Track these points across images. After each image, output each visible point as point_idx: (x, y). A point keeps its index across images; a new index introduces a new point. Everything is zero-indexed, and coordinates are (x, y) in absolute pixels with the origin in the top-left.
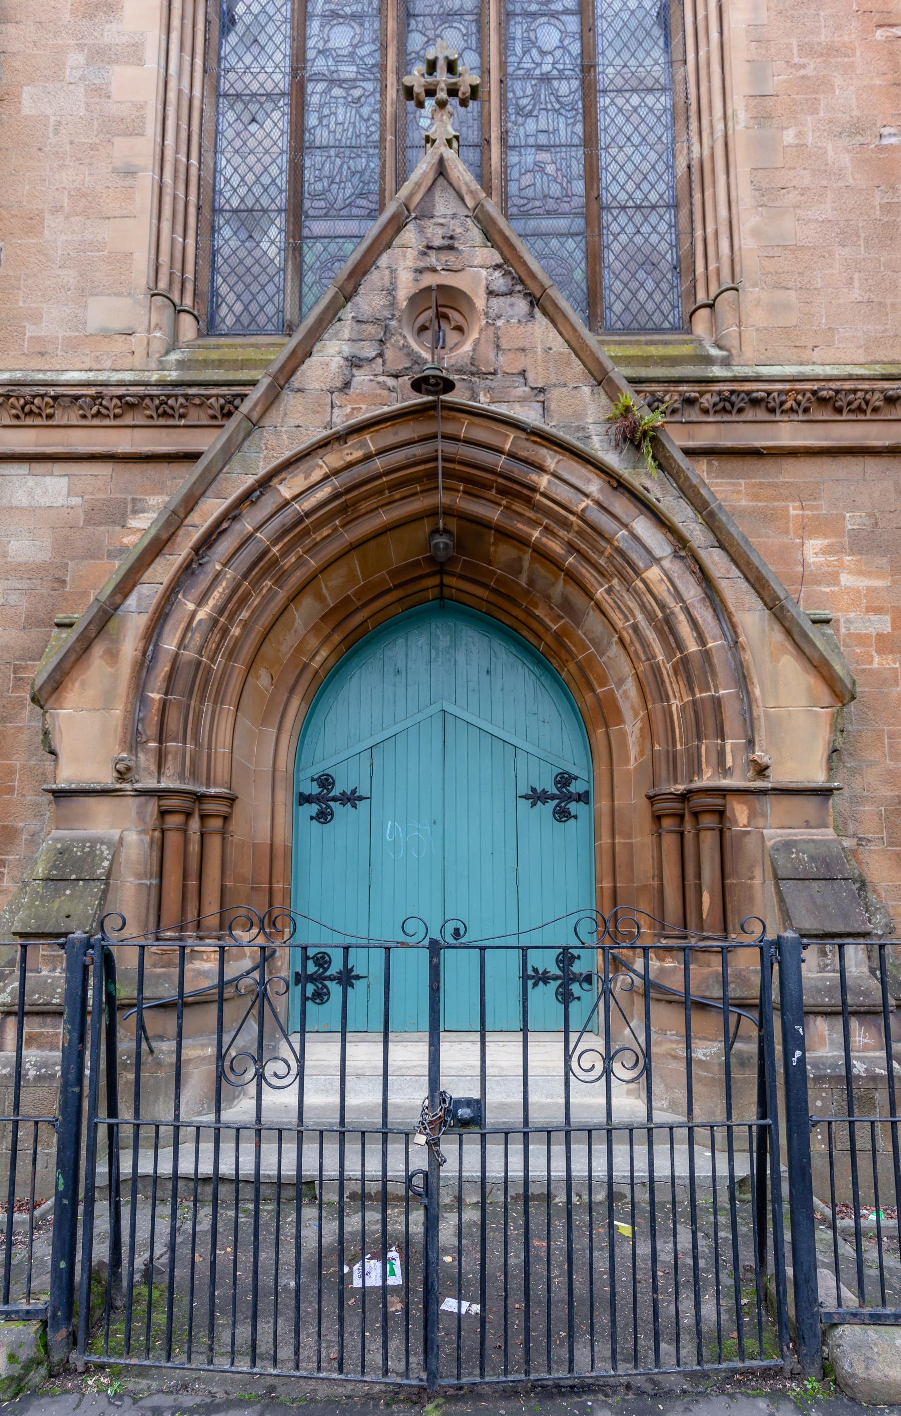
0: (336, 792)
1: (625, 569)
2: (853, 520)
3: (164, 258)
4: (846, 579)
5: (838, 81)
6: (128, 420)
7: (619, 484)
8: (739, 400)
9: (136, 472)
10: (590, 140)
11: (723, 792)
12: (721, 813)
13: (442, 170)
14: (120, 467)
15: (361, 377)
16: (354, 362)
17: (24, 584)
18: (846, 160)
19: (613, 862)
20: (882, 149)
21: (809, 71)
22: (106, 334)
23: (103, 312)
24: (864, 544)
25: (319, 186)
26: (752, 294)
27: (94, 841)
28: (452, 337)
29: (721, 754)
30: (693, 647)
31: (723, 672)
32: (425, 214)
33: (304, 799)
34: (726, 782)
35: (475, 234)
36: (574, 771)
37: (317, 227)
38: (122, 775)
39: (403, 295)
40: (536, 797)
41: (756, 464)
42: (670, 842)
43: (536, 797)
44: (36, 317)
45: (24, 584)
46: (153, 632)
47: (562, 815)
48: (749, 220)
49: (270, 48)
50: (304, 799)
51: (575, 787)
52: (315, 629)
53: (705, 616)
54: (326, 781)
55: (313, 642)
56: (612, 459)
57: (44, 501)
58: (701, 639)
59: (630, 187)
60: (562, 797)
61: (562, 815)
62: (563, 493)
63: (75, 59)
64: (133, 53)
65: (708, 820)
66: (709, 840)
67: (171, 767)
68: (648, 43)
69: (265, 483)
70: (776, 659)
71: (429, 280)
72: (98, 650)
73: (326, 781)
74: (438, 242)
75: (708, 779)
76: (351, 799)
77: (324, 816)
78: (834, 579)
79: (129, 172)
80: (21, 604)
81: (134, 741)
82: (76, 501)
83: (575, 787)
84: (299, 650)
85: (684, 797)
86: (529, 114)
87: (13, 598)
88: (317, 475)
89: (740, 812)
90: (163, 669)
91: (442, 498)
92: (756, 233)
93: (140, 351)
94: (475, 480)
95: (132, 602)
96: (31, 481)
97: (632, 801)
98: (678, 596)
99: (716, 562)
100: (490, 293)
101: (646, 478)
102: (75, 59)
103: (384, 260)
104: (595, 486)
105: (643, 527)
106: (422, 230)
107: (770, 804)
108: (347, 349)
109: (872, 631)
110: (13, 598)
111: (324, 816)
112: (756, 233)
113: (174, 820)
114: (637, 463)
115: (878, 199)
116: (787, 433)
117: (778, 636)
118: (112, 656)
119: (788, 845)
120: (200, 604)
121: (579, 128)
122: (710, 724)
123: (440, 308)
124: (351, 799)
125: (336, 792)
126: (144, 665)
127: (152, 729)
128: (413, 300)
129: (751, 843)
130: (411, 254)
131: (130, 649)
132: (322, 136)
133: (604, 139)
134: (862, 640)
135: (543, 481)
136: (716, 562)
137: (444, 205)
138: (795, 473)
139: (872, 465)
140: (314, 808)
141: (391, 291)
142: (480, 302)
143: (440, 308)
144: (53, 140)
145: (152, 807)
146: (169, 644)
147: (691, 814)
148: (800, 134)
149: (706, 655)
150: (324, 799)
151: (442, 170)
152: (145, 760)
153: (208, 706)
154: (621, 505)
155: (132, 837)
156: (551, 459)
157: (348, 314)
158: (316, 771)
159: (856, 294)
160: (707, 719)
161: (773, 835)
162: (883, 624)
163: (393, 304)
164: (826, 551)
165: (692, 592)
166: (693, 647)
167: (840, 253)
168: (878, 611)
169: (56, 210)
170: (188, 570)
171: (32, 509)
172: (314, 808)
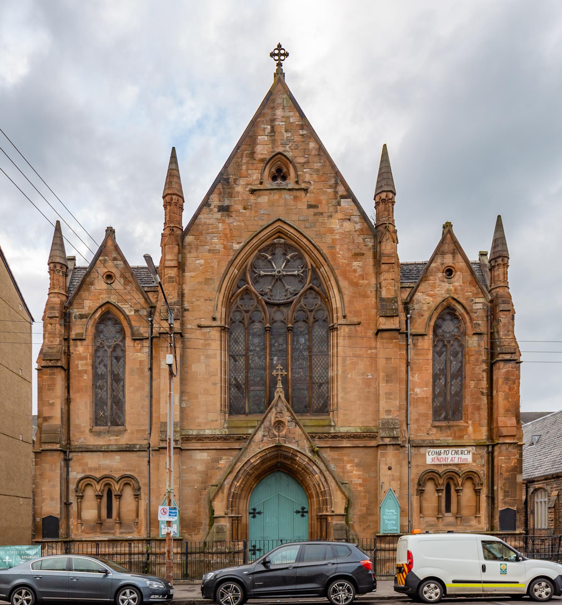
0: (256, 512)
1: (312, 474)
2: (356, 460)
3: (222, 403)
4: (354, 472)
5: (360, 363)
6: (218, 441)
7: (310, 460)
8: (335, 437)
9: (221, 452)
10: (310, 367)
11: (327, 515)
12: (326, 519)
13: (280, 397)
14: (217, 451)
15: (265, 438)
16: (264, 436)
17: (200, 475)
18: (360, 381)
19: (311, 526)
20: (368, 379)
21: (354, 360)
22: (212, 421)
23: (212, 416)
24: (358, 465)
25: (252, 378)
26: (340, 411)
27: (222, 525)
28: (281, 428)
29: (327, 508)
30: (323, 490)
31: (328, 494)
32: (277, 405)
33: (250, 513)
34: (327, 514)
35: (286, 409)
36: (305, 506)
37: (252, 388)
38: (226, 514)
39: (272, 423)
40: (298, 512)
41: (339, 449)
42: (319, 523)
43: (298, 512)
44: (198, 418)
45: (200, 475)
46: (230, 489)
47: (303, 516)
48: (340, 395)
49: (240, 344)
50: (250, 513)
51: (305, 510)
52: (254, 480)
53: (325, 484)
54: (254, 509)
55: (253, 483)
56: (310, 455)
57: (203, 458)
58: (324, 488)
59: (322, 359)
60: (303, 512)
61: (303, 516)
62: (301, 461)
63: (203, 358)
64: (215, 356)
65: (325, 520)
66: (324, 523)
67: (234, 512)
68: (324, 342)
69: (248, 460)
70: (337, 491)
71: (277, 419)
72: (220, 492)
73: (254, 509)
74: (279, 411)
75: (324, 513)
76: (259, 513)
77: (254, 517)
78: (352, 472)
79: (215, 384)
80: (200, 479)
81: (227, 508)
82: (209, 458)
83: (305, 510)
84: (250, 484)
85: (321, 515)
86: (297, 360)
87: (198, 478)
88: (257, 458)
89: (329, 519)
90: (232, 494)
91: (279, 460)
92: (342, 398)
93: (219, 425)
94: (286, 457)
95: (226, 482)
96: (200, 454)
97: (314, 514)
98: (321, 480)
99: (327, 474)
100: (289, 422)
101: (316, 458)
102: (203, 358)
103: (269, 415)
104: (307, 460)
105: (315, 467)
106: (276, 409)
107: (334, 517)
108: (262, 433)
109: (358, 482)
110: (198, 478)
111: (254, 517)
112: (342, 398)
113: (234, 521)
114: (314, 455)
115: (367, 390)
116: (345, 443)
117: (337, 487)
118: (223, 492)
119: (336, 524)
120: (238, 482)
121: (308, 364)
122: (325, 503)
123: (279, 424)
124: (259, 513)
125: (256, 512)
126: (229, 494)
127: (230, 506)
128: (275, 423)
129: (331, 524)
130: (274, 414)
131: (226, 491)
132: (252, 365)
133: (313, 366)
134: (356, 484)
135: (298, 459)
136: (327, 474)
137: (280, 404)
138: (345, 451)
139: (361, 449)
140: (252, 515)
141: (270, 422)
142: (286, 424)
143: (279, 424)
144: (199, 377)
145: (231, 519)
146: (233, 491)
147: (323, 519)
148: (352, 375)
149: (325, 491)
150: (254, 513)
151: (280, 397)
152: (229, 511)
153: (238, 500)
154: (311, 463)
155: (228, 524)
156: (299, 455)
157: (263, 426)
158: (252, 507)
159: (360, 412)
160: (325, 502)
161: (334, 522)
162: (360, 481)
163: (271, 424)
164: (351, 467)
165: (323, 480)
166: (323, 490)
167: (358, 402)
168: (360, 478)
169: (201, 394)
170: (236, 477)
171: (201, 460)
172: (252, 515)
